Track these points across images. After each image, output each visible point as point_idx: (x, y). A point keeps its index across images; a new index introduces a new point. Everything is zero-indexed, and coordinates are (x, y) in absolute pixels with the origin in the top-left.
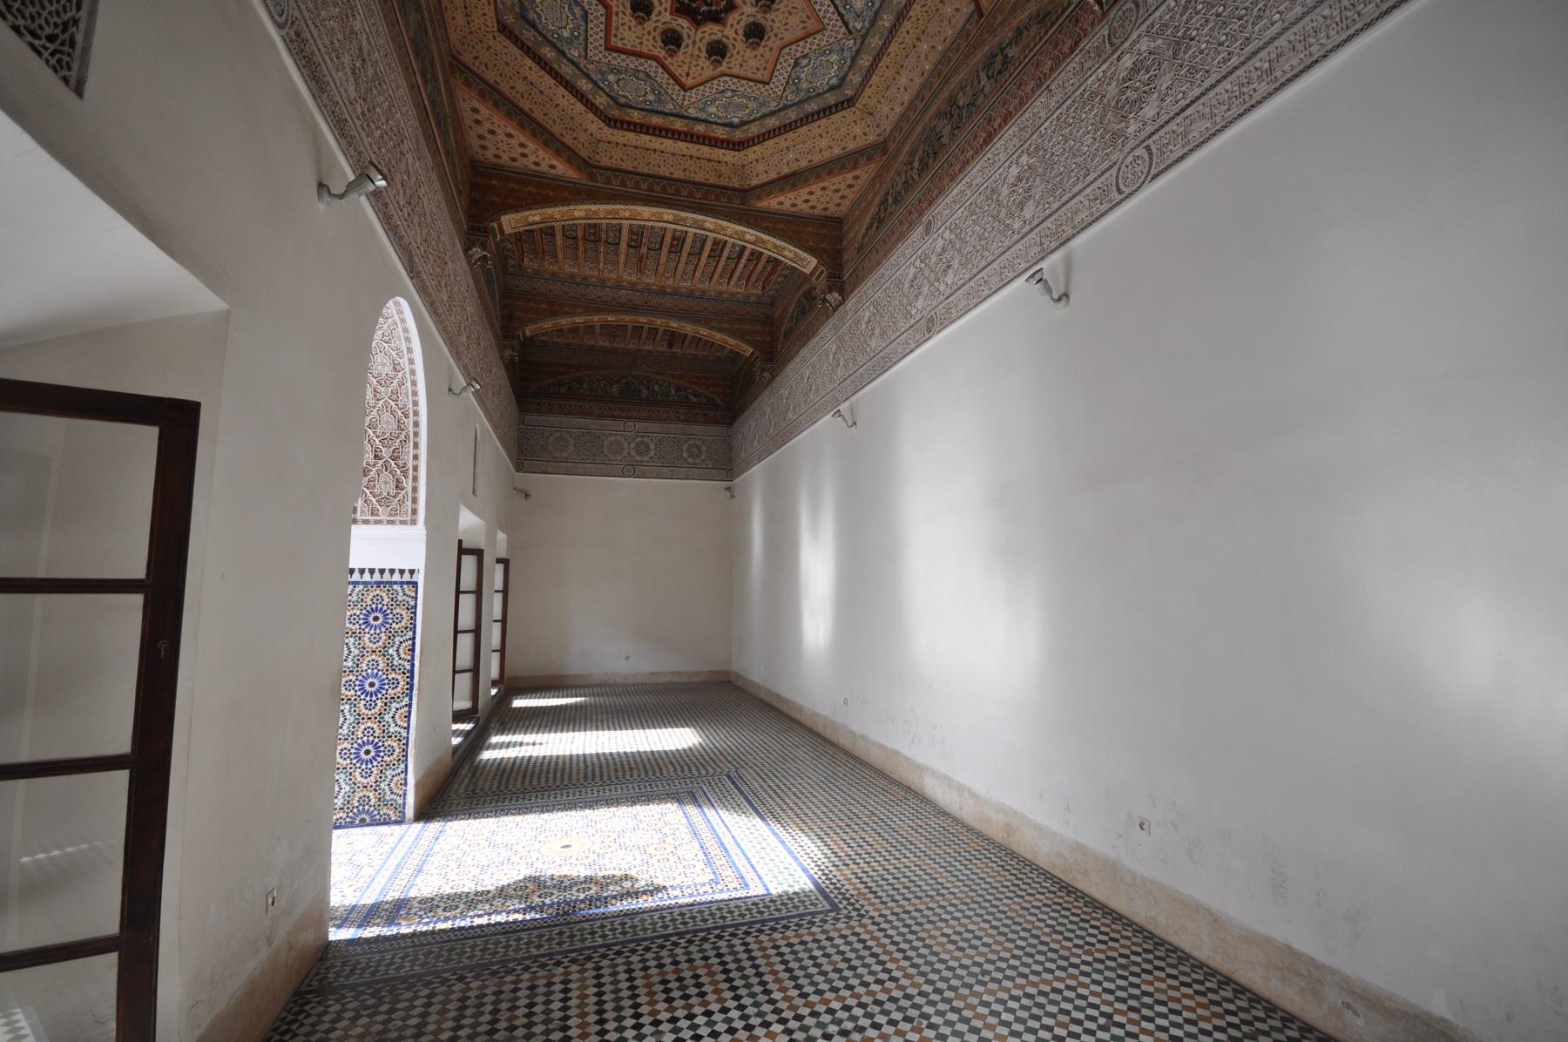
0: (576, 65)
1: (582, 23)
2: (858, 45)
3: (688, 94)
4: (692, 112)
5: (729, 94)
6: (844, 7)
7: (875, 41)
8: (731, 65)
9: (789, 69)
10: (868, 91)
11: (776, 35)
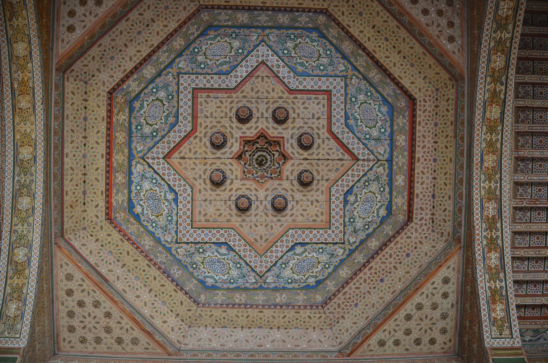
0: (170, 65)
1: (214, 71)
2: (252, 287)
3: (162, 161)
4: (138, 169)
5: (170, 196)
6: (283, 263)
7: (260, 298)
8: (203, 192)
9: (214, 240)
10: (218, 313)
11: (243, 221)
